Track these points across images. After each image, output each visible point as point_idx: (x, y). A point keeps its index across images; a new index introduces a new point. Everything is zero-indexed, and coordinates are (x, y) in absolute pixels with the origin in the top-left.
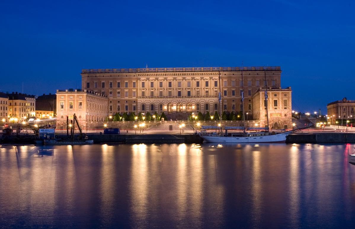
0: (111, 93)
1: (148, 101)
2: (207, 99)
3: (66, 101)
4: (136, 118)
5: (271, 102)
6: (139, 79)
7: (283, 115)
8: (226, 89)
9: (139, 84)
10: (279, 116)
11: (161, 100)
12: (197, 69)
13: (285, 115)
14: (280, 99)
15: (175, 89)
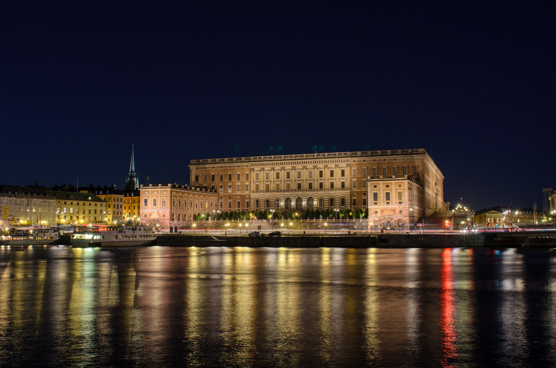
0: (221, 187)
1: (262, 196)
2: (333, 193)
3: (159, 197)
4: (331, 216)
5: (382, 195)
6: (253, 170)
7: (397, 212)
8: (355, 180)
9: (252, 176)
10: (392, 213)
11: (278, 194)
12: (341, 154)
13: (401, 212)
14: (394, 191)
15: (293, 181)
